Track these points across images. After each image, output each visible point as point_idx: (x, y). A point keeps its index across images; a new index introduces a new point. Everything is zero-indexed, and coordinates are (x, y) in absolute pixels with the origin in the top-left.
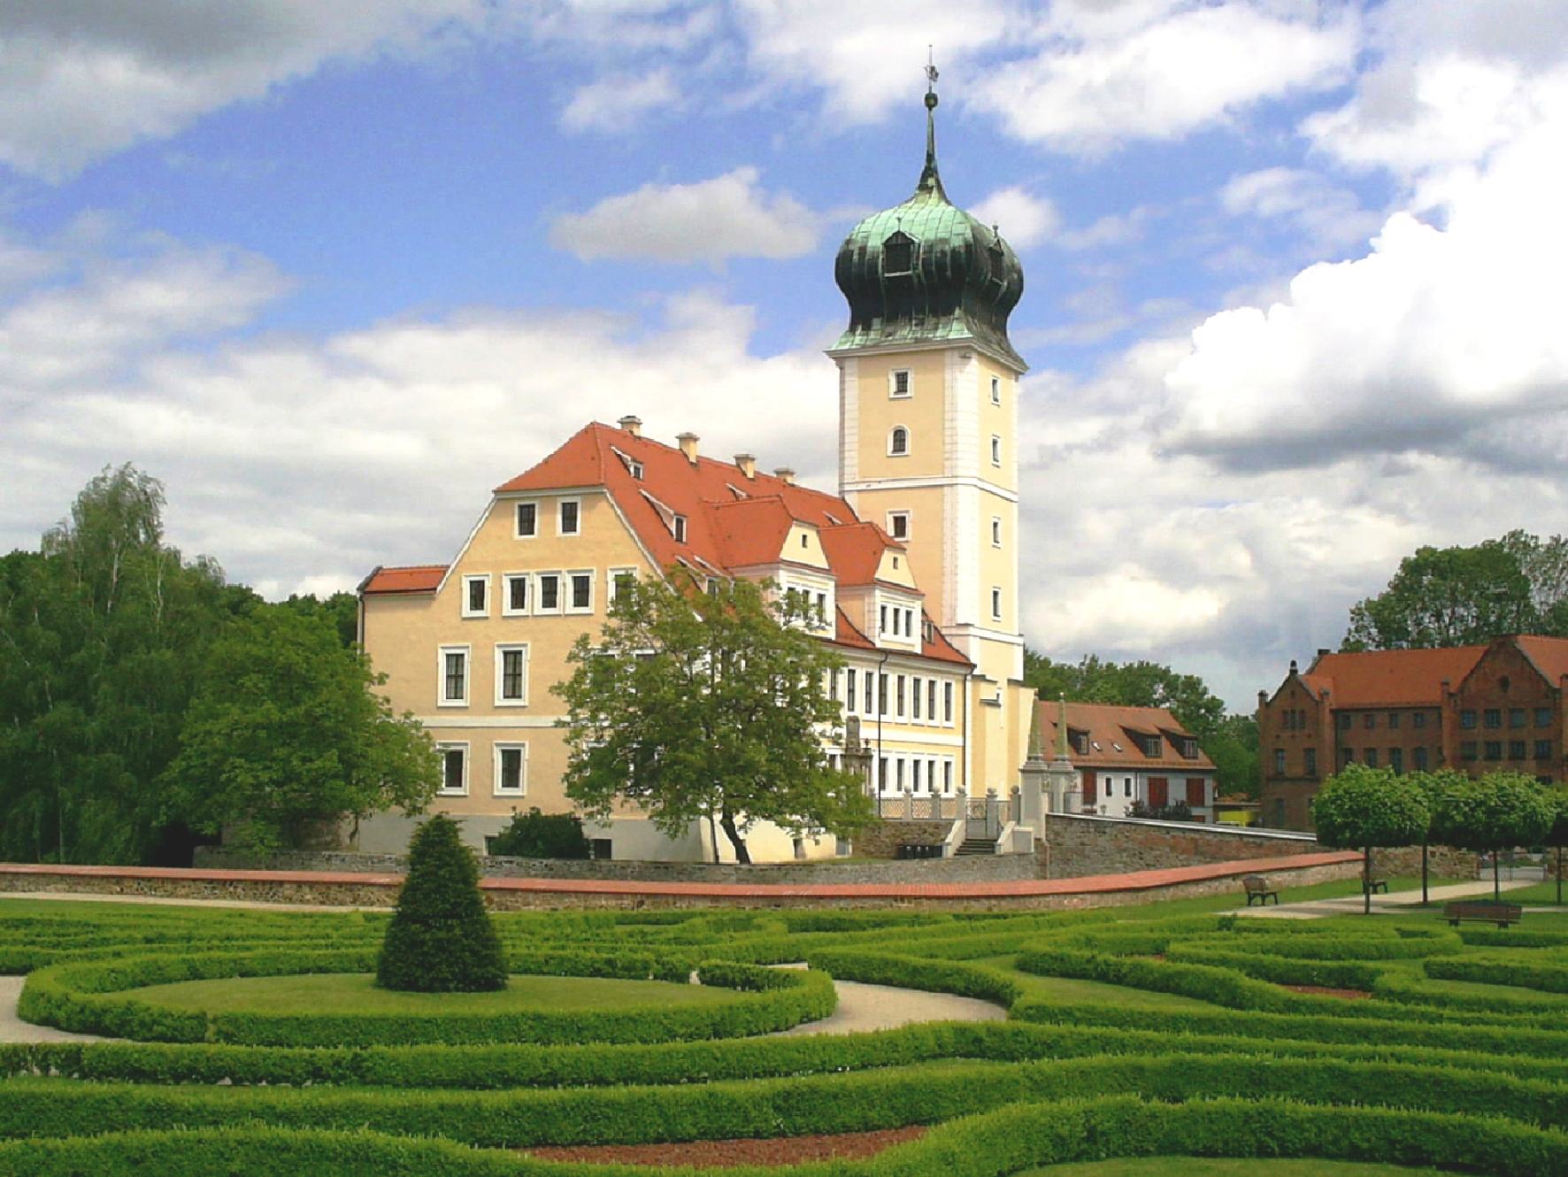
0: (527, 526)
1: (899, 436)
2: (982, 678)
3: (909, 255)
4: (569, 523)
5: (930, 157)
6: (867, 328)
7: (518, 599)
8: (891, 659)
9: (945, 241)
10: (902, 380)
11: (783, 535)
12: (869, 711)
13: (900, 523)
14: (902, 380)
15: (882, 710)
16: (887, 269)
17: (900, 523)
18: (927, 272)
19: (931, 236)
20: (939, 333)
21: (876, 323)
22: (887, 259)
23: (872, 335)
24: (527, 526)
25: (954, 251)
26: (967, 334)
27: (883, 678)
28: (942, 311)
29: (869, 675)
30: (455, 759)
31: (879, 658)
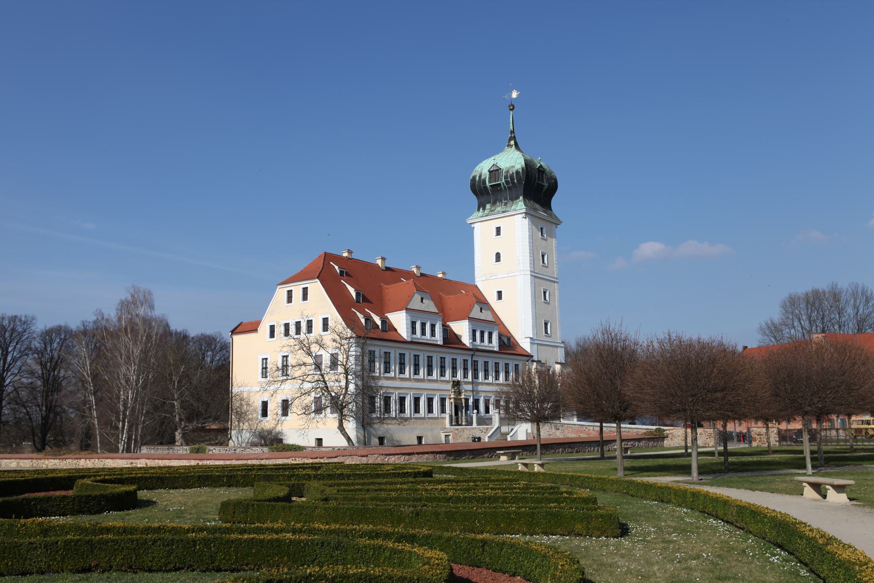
0: (290, 300)
1: (498, 257)
2: (538, 362)
3: (499, 175)
4: (305, 297)
6: (484, 209)
7: (287, 333)
8: (477, 353)
9: (513, 167)
10: (498, 230)
12: (465, 376)
13: (500, 294)
14: (498, 230)
15: (476, 376)
16: (490, 182)
17: (500, 294)
18: (507, 182)
20: (513, 207)
21: (488, 206)
22: (490, 178)
23: (486, 212)
24: (290, 300)
25: (517, 172)
26: (524, 206)
27: (475, 363)
28: (514, 199)
29: (465, 361)
30: (265, 405)
31: (472, 353)
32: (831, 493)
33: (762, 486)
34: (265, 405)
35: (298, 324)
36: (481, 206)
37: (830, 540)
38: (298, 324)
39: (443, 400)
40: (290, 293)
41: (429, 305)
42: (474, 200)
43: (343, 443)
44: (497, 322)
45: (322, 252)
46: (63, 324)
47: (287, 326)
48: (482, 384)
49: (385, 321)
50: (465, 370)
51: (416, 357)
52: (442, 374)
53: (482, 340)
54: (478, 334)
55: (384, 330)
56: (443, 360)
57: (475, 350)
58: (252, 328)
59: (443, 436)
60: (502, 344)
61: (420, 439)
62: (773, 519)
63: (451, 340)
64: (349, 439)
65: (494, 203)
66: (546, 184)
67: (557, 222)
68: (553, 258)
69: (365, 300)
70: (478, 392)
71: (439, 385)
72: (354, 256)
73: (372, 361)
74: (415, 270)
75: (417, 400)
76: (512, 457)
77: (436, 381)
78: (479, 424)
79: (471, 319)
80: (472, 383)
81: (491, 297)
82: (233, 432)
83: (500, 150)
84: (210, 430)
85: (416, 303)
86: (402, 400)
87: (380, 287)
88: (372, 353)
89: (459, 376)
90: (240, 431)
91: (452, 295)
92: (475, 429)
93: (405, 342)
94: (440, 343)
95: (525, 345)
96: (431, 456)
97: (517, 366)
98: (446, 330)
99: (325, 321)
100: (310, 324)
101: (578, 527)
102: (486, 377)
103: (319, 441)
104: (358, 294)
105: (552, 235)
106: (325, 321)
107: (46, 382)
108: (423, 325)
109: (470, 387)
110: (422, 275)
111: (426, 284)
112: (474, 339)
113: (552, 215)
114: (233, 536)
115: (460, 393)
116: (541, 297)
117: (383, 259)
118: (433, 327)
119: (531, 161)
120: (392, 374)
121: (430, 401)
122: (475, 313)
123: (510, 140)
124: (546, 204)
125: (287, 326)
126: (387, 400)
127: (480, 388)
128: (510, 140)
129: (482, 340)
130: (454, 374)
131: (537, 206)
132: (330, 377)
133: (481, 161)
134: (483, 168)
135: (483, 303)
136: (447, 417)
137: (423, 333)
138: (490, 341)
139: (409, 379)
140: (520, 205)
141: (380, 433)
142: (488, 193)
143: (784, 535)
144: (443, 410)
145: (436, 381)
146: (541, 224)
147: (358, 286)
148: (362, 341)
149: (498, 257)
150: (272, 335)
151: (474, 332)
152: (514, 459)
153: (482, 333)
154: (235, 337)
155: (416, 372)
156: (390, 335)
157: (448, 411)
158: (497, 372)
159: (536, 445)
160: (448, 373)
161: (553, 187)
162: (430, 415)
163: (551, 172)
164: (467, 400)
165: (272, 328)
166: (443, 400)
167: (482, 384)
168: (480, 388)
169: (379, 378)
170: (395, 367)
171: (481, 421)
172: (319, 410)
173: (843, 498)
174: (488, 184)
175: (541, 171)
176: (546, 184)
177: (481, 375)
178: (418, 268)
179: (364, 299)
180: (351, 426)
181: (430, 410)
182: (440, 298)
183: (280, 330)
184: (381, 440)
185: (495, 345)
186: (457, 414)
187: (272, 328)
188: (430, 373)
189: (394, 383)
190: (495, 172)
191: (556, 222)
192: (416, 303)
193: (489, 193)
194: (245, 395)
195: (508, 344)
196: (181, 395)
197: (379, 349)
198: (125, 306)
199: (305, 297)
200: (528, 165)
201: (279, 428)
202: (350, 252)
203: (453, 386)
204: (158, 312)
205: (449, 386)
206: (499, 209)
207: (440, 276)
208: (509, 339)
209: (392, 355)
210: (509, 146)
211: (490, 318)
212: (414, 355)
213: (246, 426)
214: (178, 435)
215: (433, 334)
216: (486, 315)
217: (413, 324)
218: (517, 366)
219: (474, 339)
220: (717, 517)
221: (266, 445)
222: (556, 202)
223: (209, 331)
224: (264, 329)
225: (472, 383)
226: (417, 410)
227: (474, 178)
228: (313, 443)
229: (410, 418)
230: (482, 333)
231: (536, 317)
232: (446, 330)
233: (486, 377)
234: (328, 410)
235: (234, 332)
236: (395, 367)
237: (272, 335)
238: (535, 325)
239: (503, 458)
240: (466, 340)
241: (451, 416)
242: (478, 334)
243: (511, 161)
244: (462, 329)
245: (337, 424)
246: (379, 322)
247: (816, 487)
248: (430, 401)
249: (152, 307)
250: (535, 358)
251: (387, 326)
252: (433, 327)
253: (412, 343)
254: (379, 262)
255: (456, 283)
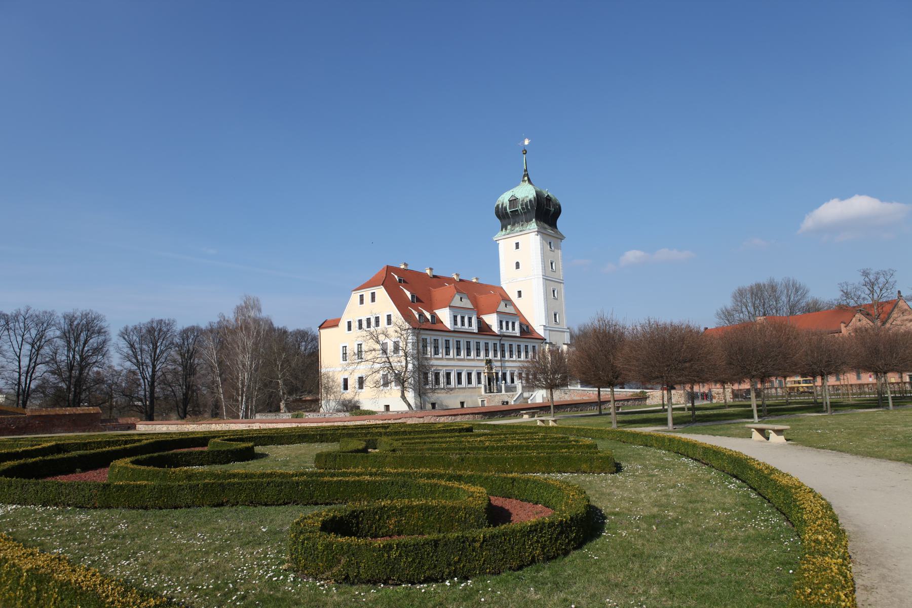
0: (362, 302)
2: (550, 343)
4: (373, 299)
5: (526, 170)
7: (360, 327)
10: (517, 245)
11: (452, 298)
12: (495, 356)
13: (520, 292)
14: (517, 245)
15: (503, 356)
17: (520, 292)
18: (523, 209)
19: (523, 196)
21: (509, 227)
24: (362, 302)
25: (530, 201)
27: (502, 346)
28: (528, 221)
30: (346, 381)
32: (773, 436)
33: (721, 432)
34: (346, 381)
35: (369, 320)
36: (504, 227)
37: (773, 471)
38: (369, 320)
39: (479, 374)
40: (362, 296)
41: (467, 303)
42: (498, 223)
43: (405, 408)
44: (518, 314)
45: (383, 266)
46: (195, 324)
47: (360, 321)
48: (508, 361)
49: (434, 316)
50: (495, 351)
51: (458, 342)
52: (478, 354)
53: (507, 329)
54: (504, 324)
55: (433, 323)
56: (478, 344)
57: (502, 336)
58: (335, 324)
59: (480, 401)
60: (522, 331)
61: (462, 403)
62: (730, 456)
63: (484, 329)
64: (409, 405)
65: (514, 225)
66: (552, 209)
67: (561, 238)
68: (559, 265)
69: (419, 300)
70: (505, 367)
71: (476, 363)
72: (409, 268)
73: (425, 346)
74: (455, 277)
75: (459, 375)
76: (533, 415)
77: (473, 360)
78: (506, 391)
79: (498, 313)
80: (501, 361)
81: (513, 296)
82: (323, 402)
83: (516, 184)
84: (306, 401)
85: (456, 302)
86: (448, 375)
87: (429, 290)
88: (425, 340)
89: (491, 356)
90: (328, 401)
91: (483, 294)
92: (504, 395)
93: (450, 331)
94: (476, 331)
95: (540, 331)
96: (471, 416)
97: (534, 347)
98: (480, 322)
99: (389, 317)
100: (377, 319)
101: (584, 466)
102: (511, 356)
103: (387, 407)
104: (413, 296)
105: (558, 248)
106: (389, 317)
107: (185, 368)
108: (463, 318)
109: (499, 364)
110: (461, 280)
111: (463, 287)
112: (501, 328)
113: (557, 232)
114: (326, 479)
115: (492, 369)
116: (551, 294)
117: (431, 269)
118: (470, 319)
119: (541, 192)
120: (440, 356)
121: (469, 375)
122: (502, 307)
123: (524, 176)
124: (553, 225)
125: (360, 321)
126: (437, 375)
127: (507, 364)
128: (524, 176)
129: (507, 329)
130: (487, 354)
131: (546, 226)
132: (394, 359)
133: (503, 193)
134: (504, 199)
135: (508, 301)
136: (483, 386)
137: (463, 324)
138: (513, 329)
139: (453, 359)
140: (533, 225)
141: (433, 400)
142: (509, 217)
143: (738, 468)
144: (479, 382)
145: (473, 360)
146: (549, 239)
147: (413, 291)
148: (417, 331)
149: (517, 265)
150: (349, 328)
151: (501, 322)
152: (533, 417)
153: (507, 323)
154: (322, 331)
155: (458, 354)
156: (438, 326)
157: (483, 382)
158: (519, 352)
159: (550, 407)
160: (482, 353)
161: (558, 212)
162: (470, 386)
163: (556, 200)
164: (497, 374)
165: (349, 323)
166: (479, 374)
167: (508, 361)
168: (507, 364)
169: (430, 359)
170: (442, 351)
171: (508, 389)
172: (386, 384)
173: (781, 439)
174: (508, 210)
175: (548, 199)
176: (552, 209)
177: (507, 354)
178: (457, 275)
179: (417, 300)
180: (410, 395)
181: (470, 382)
182: (475, 297)
183: (355, 325)
184: (433, 405)
185: (517, 332)
186: (489, 384)
187: (349, 323)
188: (469, 354)
189: (441, 362)
190: (513, 201)
191: (561, 238)
192: (456, 302)
193: (509, 217)
194: (331, 374)
195: (527, 331)
196: (284, 375)
197: (430, 337)
198: (240, 310)
199: (373, 299)
200: (539, 195)
201: (356, 398)
202: (406, 265)
203: (487, 363)
204: (264, 314)
205: (483, 364)
206: (517, 229)
207: (474, 280)
208: (527, 327)
209: (440, 342)
210: (524, 181)
211: (512, 311)
212: (457, 341)
213: (332, 397)
214: (282, 405)
215: (470, 325)
216: (510, 310)
217: (455, 317)
218: (534, 347)
219: (501, 328)
220: (688, 456)
221: (347, 411)
222: (560, 222)
223: (302, 327)
224: (343, 324)
225: (501, 361)
226: (460, 382)
227: (498, 206)
228: (383, 409)
229: (455, 388)
230: (507, 323)
231: (547, 309)
232: (480, 322)
233: (511, 356)
234: (393, 383)
235: (321, 327)
236: (442, 351)
237: (349, 328)
238: (547, 316)
239: (526, 417)
240: (495, 328)
241: (485, 386)
242: (504, 324)
243: (525, 192)
244: (492, 320)
245: (400, 394)
246: (429, 317)
247: (762, 431)
248: (469, 375)
249: (260, 310)
250: (548, 341)
251: (436, 320)
252: (470, 319)
253: (454, 332)
254: (428, 272)
255: (487, 286)
